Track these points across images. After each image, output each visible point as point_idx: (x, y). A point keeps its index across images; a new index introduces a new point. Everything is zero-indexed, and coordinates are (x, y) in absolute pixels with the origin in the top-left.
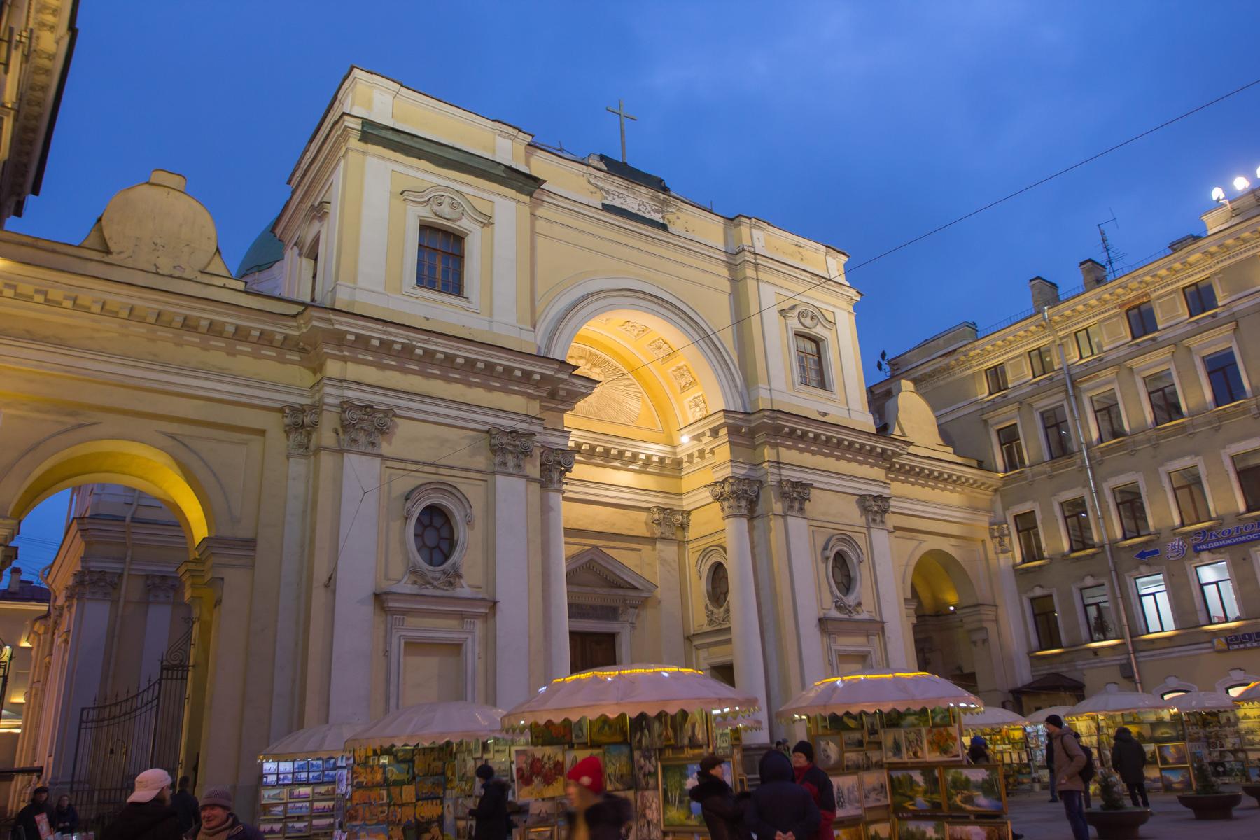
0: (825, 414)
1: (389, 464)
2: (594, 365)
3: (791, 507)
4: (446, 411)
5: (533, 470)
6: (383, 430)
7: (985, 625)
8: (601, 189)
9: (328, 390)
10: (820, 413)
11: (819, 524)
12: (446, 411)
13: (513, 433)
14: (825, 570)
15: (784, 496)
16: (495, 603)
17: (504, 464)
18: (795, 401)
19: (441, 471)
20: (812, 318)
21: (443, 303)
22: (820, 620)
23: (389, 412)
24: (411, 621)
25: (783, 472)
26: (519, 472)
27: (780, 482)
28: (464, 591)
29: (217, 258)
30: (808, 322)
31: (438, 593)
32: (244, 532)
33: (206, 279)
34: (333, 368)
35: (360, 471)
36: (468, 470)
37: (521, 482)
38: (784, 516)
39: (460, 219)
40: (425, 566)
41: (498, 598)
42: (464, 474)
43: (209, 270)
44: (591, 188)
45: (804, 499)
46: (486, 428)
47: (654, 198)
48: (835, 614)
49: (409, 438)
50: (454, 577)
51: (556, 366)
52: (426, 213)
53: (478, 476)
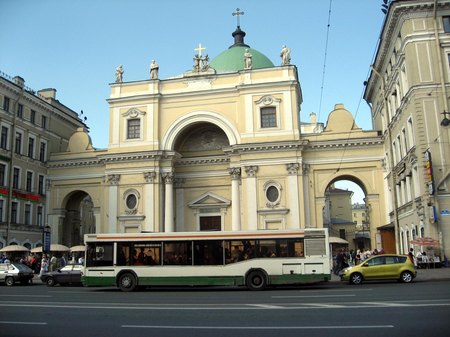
2: (214, 132)
5: (157, 180)
6: (118, 179)
7: (370, 203)
9: (106, 172)
11: (262, 178)
14: (263, 194)
15: (247, 171)
18: (256, 135)
20: (270, 100)
22: (257, 212)
24: (126, 222)
28: (138, 214)
29: (90, 145)
30: (268, 103)
31: (132, 215)
32: (98, 206)
35: (113, 190)
39: (137, 115)
40: (128, 209)
43: (89, 148)
48: (266, 209)
49: (124, 180)
50: (135, 212)
52: (128, 117)
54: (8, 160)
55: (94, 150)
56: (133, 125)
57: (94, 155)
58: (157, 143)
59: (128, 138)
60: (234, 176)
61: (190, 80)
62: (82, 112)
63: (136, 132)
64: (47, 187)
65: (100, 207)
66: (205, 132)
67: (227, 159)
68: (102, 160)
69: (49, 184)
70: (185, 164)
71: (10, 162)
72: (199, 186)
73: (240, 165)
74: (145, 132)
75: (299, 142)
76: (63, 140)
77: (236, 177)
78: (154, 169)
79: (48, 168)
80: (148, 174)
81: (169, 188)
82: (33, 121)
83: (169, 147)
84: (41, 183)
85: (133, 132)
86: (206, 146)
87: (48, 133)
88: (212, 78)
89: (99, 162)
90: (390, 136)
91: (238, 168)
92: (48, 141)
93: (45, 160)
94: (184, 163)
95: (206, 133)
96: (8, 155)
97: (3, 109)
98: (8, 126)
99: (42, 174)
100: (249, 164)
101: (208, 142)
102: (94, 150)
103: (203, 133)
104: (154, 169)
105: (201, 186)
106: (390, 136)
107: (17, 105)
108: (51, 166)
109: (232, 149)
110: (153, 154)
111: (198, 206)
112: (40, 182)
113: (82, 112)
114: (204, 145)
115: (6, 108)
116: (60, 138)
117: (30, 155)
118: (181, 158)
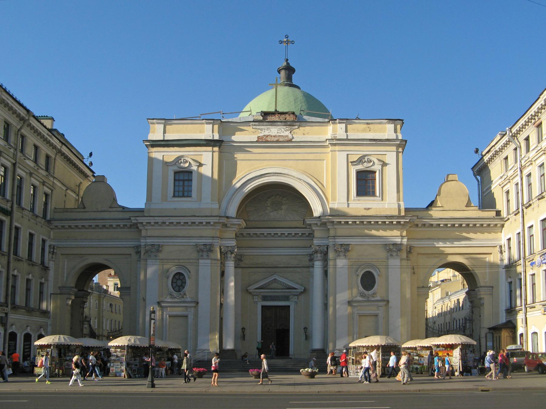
0: (369, 209)
1: (163, 261)
3: (339, 255)
4: (181, 241)
8: (259, 129)
10: (365, 209)
12: (181, 241)
13: (205, 245)
15: (336, 251)
16: (198, 303)
17: (202, 256)
19: (180, 261)
21: (182, 201)
23: (159, 245)
25: (337, 240)
26: (208, 257)
27: (334, 245)
33: (110, 210)
34: (144, 233)
36: (189, 259)
37: (209, 261)
38: (335, 259)
41: (199, 301)
42: (188, 261)
44: (254, 130)
45: (347, 250)
46: (195, 244)
47: (284, 125)
51: (218, 218)
53: (194, 261)
54: (8, 213)
55: (121, 209)
56: (182, 179)
57: (127, 215)
58: (217, 206)
59: (174, 196)
60: (319, 255)
61: (263, 125)
62: (91, 155)
63: (186, 188)
64: (51, 255)
65: (130, 288)
66: (272, 196)
67: (302, 234)
68: (136, 224)
69: (53, 252)
70: (244, 237)
71: (9, 217)
72: (262, 266)
73: (327, 242)
74: (200, 191)
75: (406, 218)
76: (68, 191)
77: (321, 257)
78: (211, 241)
79: (52, 229)
80: (202, 247)
81: (230, 265)
82: (36, 161)
83: (232, 211)
84: (43, 249)
85: (181, 189)
86: (273, 215)
87: (52, 179)
88: (293, 126)
89: (131, 225)
90: (523, 217)
91: (324, 246)
92: (52, 191)
93: (48, 218)
94: (265, 234)
95: (273, 197)
96: (8, 207)
97: (3, 138)
98: (9, 164)
99: (45, 238)
100: (340, 241)
101: (275, 210)
102: (121, 209)
103: (270, 198)
104: (211, 241)
105: (265, 266)
106: (523, 217)
107: (19, 136)
108: (56, 226)
109: (321, 221)
110: (212, 220)
111: (261, 292)
112: (42, 248)
113: (91, 155)
114: (271, 214)
115: (6, 138)
116: (64, 188)
117: (32, 210)
118: (245, 228)
